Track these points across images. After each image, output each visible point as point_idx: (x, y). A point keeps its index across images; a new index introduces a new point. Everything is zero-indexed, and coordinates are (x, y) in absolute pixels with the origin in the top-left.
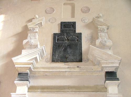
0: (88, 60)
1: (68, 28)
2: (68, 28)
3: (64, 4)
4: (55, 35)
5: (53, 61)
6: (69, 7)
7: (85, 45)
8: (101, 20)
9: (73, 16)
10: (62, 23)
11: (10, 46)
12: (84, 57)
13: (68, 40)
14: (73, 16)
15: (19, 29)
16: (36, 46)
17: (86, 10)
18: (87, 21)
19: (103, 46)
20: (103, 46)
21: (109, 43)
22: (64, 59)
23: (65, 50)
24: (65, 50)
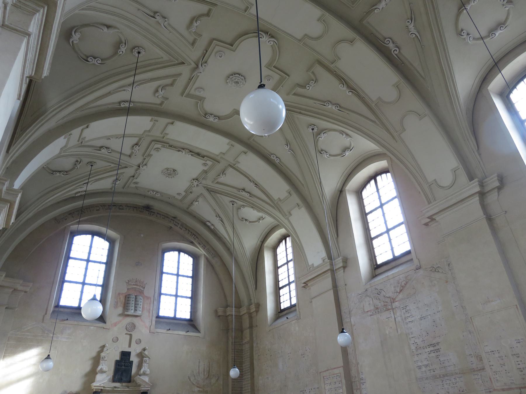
0: (134, 381)
1: (125, 355)
2: (125, 355)
3: (126, 334)
4: (117, 362)
5: (114, 381)
6: (128, 337)
7: (134, 370)
8: (146, 352)
9: (130, 346)
10: (122, 352)
11: (87, 367)
12: (132, 379)
13: (125, 366)
14: (130, 346)
15: (94, 354)
16: (105, 372)
17: (139, 342)
18: (138, 351)
19: (144, 374)
20: (144, 374)
21: (148, 372)
22: (120, 381)
23: (122, 374)
24: (122, 374)
